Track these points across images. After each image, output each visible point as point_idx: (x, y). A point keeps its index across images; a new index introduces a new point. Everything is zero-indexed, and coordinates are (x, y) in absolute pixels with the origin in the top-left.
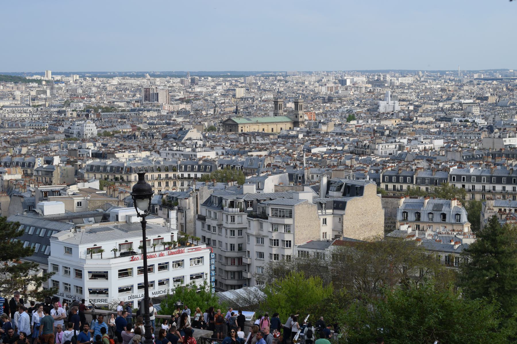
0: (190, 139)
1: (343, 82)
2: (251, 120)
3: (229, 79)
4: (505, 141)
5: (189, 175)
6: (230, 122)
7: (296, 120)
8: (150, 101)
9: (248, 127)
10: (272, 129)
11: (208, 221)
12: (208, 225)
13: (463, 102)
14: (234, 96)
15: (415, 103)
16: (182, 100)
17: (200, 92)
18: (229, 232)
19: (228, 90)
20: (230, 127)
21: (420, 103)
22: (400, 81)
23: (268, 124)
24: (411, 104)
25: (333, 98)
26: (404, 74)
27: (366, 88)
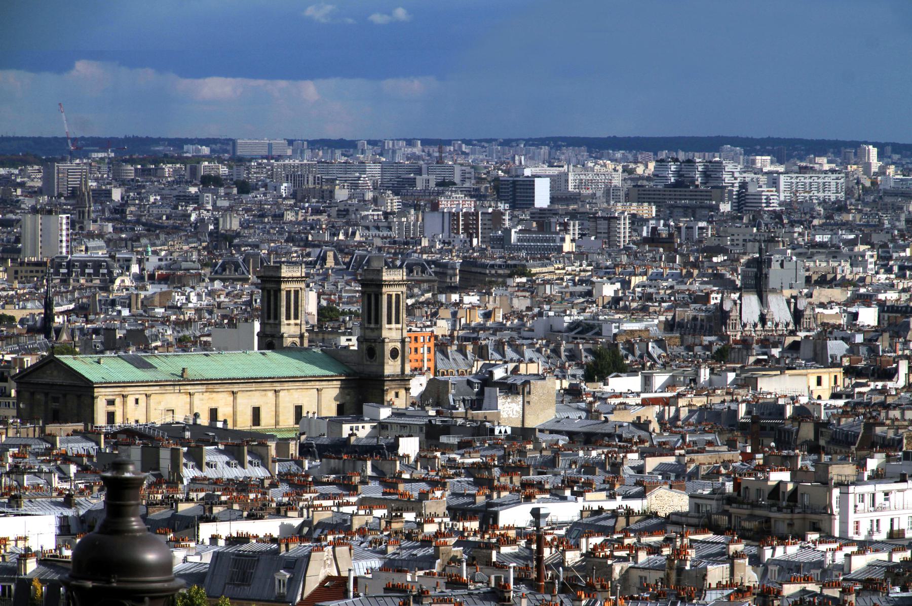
7: (370, 367)
10: (256, 412)
15: (881, 297)
23: (235, 388)
24: (866, 301)
25: (484, 266)
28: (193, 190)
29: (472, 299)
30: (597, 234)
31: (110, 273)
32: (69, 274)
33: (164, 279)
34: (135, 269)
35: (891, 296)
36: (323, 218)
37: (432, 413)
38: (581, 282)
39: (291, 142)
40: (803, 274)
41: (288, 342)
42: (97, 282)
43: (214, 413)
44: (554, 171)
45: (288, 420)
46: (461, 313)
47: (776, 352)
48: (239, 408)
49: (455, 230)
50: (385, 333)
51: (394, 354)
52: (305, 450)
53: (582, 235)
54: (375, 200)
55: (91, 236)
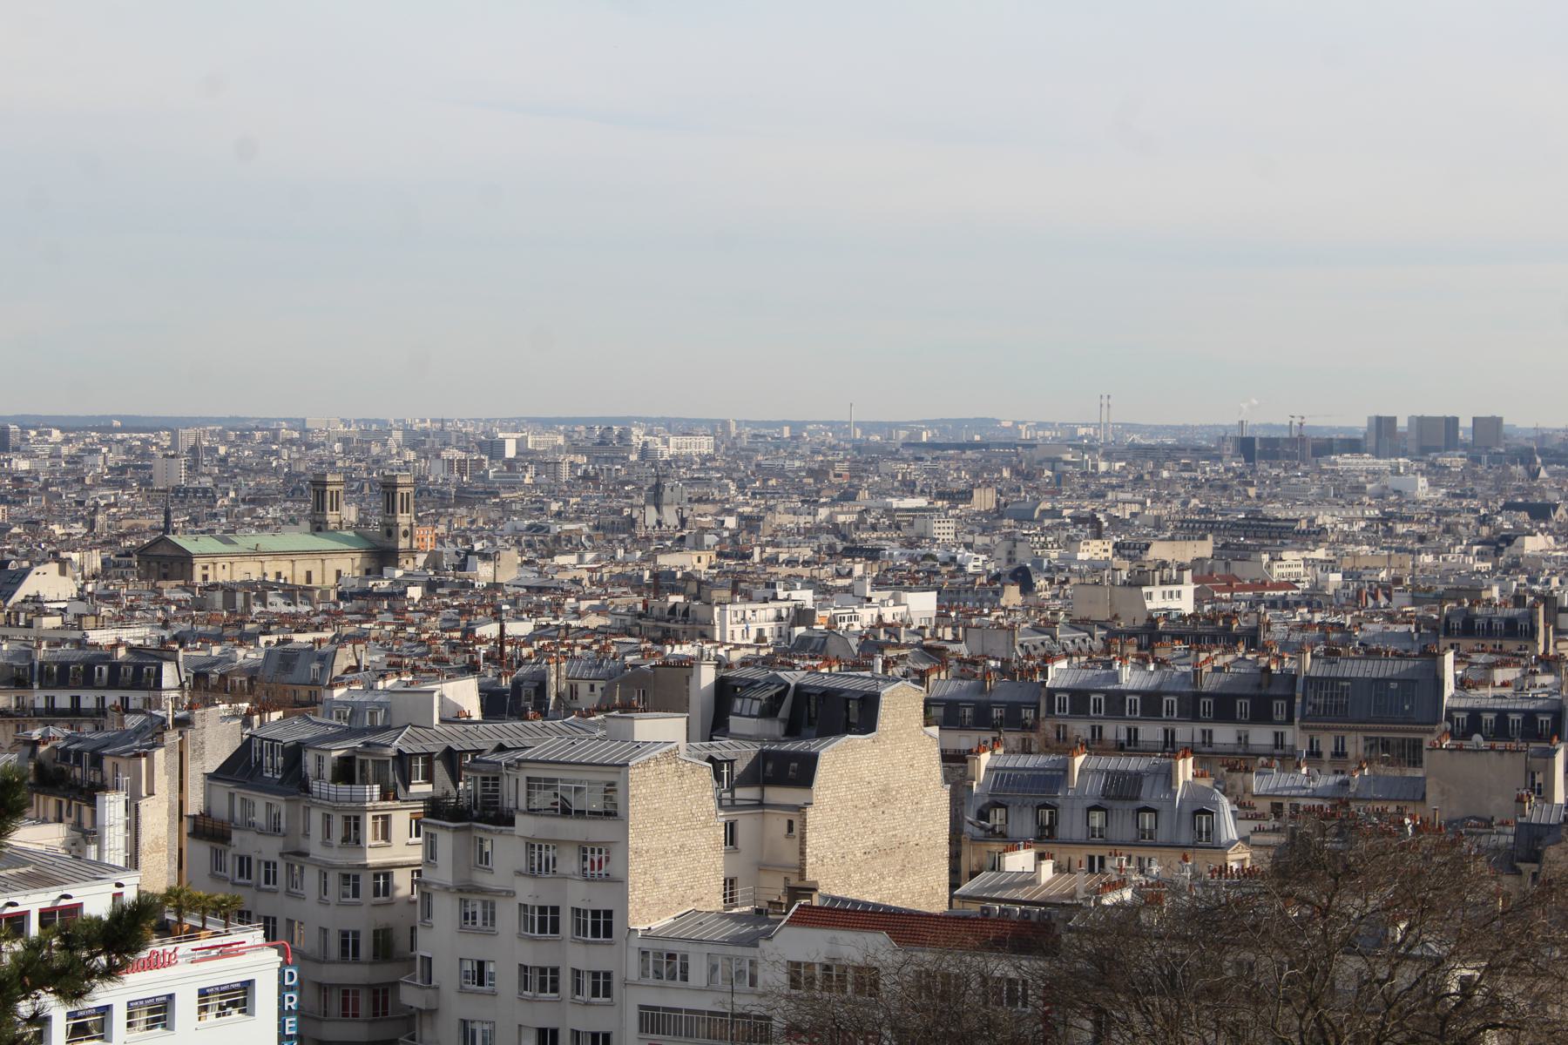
1: (494, 448)
2: (234, 543)
3: (119, 436)
5: (76, 700)
7: (389, 543)
10: (309, 574)
11: (242, 842)
13: (895, 506)
14: (146, 483)
15: (740, 510)
17: (29, 472)
18: (333, 879)
19: (122, 469)
20: (165, 566)
21: (756, 510)
22: (673, 450)
23: (294, 558)
24: (730, 512)
25: (471, 493)
28: (274, 447)
29: (463, 511)
30: (547, 473)
31: (214, 496)
32: (186, 497)
33: (252, 501)
34: (232, 494)
35: (747, 510)
36: (363, 465)
37: (431, 573)
38: (536, 502)
39: (342, 420)
40: (686, 496)
41: (331, 526)
42: (204, 501)
43: (279, 575)
44: (520, 435)
45: (331, 580)
46: (454, 520)
47: (669, 543)
48: (297, 572)
49: (451, 470)
50: (399, 520)
51: (405, 534)
52: (341, 596)
53: (537, 474)
54: (398, 454)
55: (203, 474)
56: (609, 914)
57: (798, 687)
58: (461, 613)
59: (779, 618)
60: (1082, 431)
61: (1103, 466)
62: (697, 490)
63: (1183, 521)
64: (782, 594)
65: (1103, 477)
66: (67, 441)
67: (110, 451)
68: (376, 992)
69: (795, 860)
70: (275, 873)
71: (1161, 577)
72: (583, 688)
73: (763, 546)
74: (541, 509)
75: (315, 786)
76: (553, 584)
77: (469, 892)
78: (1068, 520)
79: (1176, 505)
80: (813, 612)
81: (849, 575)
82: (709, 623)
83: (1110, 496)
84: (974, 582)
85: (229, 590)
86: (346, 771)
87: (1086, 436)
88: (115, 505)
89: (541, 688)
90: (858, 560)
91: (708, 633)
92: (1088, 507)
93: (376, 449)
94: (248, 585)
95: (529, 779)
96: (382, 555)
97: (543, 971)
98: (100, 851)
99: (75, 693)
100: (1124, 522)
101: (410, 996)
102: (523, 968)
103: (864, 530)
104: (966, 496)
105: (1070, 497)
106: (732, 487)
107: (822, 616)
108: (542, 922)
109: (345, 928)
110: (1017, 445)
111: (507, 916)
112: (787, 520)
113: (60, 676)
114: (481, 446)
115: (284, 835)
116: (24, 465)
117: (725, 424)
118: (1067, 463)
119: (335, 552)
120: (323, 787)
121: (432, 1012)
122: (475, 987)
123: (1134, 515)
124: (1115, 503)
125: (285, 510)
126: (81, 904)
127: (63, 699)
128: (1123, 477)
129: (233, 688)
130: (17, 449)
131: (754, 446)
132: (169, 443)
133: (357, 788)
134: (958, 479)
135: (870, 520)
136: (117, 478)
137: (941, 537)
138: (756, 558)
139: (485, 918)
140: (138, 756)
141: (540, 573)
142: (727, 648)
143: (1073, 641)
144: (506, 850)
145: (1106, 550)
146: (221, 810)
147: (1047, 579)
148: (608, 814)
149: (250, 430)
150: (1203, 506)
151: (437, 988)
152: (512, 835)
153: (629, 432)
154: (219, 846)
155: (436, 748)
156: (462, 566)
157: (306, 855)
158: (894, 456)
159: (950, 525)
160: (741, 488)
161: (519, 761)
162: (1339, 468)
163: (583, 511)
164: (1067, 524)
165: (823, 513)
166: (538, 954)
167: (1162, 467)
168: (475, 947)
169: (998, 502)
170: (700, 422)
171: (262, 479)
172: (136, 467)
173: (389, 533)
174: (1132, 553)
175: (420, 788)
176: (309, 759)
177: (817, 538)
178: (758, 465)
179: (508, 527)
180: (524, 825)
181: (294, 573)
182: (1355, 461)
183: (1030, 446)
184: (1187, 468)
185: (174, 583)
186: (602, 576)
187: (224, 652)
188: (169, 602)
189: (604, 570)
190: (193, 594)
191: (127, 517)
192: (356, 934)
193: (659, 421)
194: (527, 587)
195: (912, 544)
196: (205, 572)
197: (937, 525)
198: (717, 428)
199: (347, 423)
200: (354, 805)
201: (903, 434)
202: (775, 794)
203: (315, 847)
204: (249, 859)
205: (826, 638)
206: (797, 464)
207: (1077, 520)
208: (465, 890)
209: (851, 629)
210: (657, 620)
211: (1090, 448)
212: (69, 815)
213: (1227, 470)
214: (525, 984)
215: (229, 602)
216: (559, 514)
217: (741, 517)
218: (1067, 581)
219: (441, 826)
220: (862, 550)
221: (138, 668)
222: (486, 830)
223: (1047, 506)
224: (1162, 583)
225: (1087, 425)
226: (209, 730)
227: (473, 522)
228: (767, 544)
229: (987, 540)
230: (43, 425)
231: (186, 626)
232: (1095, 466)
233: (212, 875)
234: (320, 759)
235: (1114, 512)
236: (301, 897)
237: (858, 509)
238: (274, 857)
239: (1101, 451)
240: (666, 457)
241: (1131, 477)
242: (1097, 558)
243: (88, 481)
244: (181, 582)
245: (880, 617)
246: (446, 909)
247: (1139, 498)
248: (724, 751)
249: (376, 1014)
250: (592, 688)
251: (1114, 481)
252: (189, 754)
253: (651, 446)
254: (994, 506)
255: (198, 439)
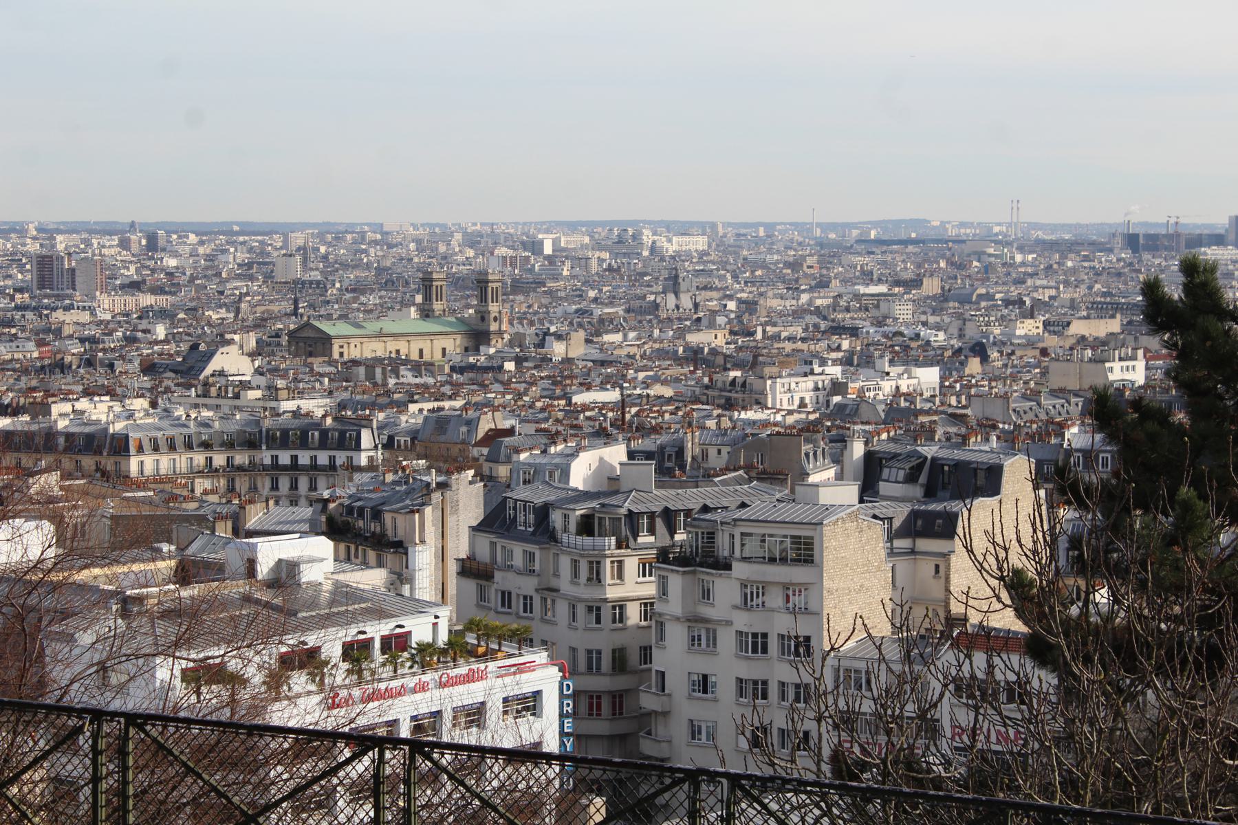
0: (222, 373)
1: (536, 247)
2: (363, 327)
3: (241, 239)
4: (1111, 370)
5: (294, 458)
6: (311, 334)
7: (482, 327)
8: (52, 289)
9: (359, 345)
10: (421, 351)
11: (502, 580)
12: (503, 593)
13: (862, 292)
14: (268, 277)
15: (738, 296)
16: (135, 286)
17: (177, 268)
18: (581, 610)
19: (249, 265)
20: (310, 346)
21: (751, 296)
22: (675, 247)
23: (409, 338)
24: (730, 298)
25: (523, 283)
26: (684, 229)
27: (601, 260)
28: (364, 247)
29: (520, 298)
30: (580, 267)
31: (325, 287)
32: (303, 287)
33: (354, 291)
34: (338, 285)
35: (744, 295)
36: (434, 260)
37: (518, 350)
38: (576, 290)
39: (412, 224)
40: (695, 284)
41: (437, 313)
42: (318, 291)
43: (398, 352)
44: (554, 236)
45: (438, 356)
46: (515, 306)
47: (688, 323)
49: (505, 264)
50: (490, 308)
51: (495, 319)
52: (453, 369)
53: (572, 268)
54: (460, 251)
55: (311, 269)
56: (808, 639)
57: (934, 459)
58: (555, 383)
59: (816, 389)
60: (996, 229)
61: (1019, 258)
62: (702, 280)
63: (1093, 303)
64: (817, 369)
65: (1020, 266)
66: (202, 243)
67: (236, 250)
68: (614, 697)
69: (941, 594)
70: (531, 604)
71: (1120, 355)
72: (712, 452)
73: (764, 325)
74: (581, 296)
75: (565, 538)
76: (611, 359)
77: (696, 621)
78: (1000, 303)
79: (1083, 289)
80: (846, 384)
81: (839, 348)
82: (763, 393)
83: (1029, 282)
84: (942, 355)
85: (370, 365)
86: (587, 526)
87: (1000, 233)
88: (247, 294)
89: (680, 452)
90: (844, 336)
91: (761, 401)
92: (1014, 292)
93: (442, 248)
94: (378, 361)
95: (742, 534)
96: (478, 336)
97: (755, 682)
98: (412, 590)
99: (294, 453)
100: (1045, 303)
101: (648, 701)
102: (740, 680)
103: (841, 311)
104: (916, 283)
105: (996, 283)
106: (729, 276)
107: (853, 386)
108: (755, 645)
109: (590, 647)
110: (946, 242)
111: (727, 641)
112: (775, 303)
113: (281, 439)
114: (524, 246)
115: (539, 575)
116: (172, 262)
117: (714, 226)
118: (990, 255)
119: (441, 334)
120: (570, 538)
121: (665, 714)
122: (701, 695)
123: (1051, 298)
124: (1036, 288)
125: (380, 297)
126: (410, 632)
127: (285, 458)
128: (1035, 266)
129: (399, 446)
130: (164, 250)
131: (738, 243)
132: (281, 244)
133: (598, 540)
134: (908, 270)
135: (843, 303)
136: (246, 271)
137: (902, 317)
138: (759, 336)
139: (708, 640)
140: (413, 512)
141: (601, 350)
142: (783, 413)
143: (1054, 407)
144: (725, 589)
145: (1038, 328)
146: (484, 554)
147: (998, 351)
148: (806, 561)
149: (342, 233)
150: (1105, 290)
151: (669, 695)
152: (729, 577)
153: (641, 233)
154: (483, 583)
155: (657, 508)
156: (541, 344)
157: (557, 590)
158: (849, 250)
159: (909, 307)
160: (735, 277)
161: (735, 520)
162: (1209, 257)
163: (614, 297)
164: (999, 306)
165: (805, 298)
166: (752, 670)
167: (1066, 258)
168: (701, 664)
169: (943, 288)
170: (692, 224)
171: (358, 273)
172: (259, 263)
173: (483, 319)
174: (1056, 329)
175: (645, 539)
176: (556, 517)
177: (803, 318)
178: (745, 259)
179: (559, 310)
180: (740, 570)
181: (409, 349)
182: (1221, 252)
183: (959, 241)
184: (1086, 259)
185: (321, 359)
186: (645, 351)
187: (388, 417)
188: (322, 375)
189: (646, 347)
190: (337, 368)
191: (259, 304)
192: (599, 652)
193: (660, 223)
194: (592, 361)
195: (880, 322)
196: (341, 350)
197: (898, 307)
198: (707, 228)
199: (415, 227)
200: (596, 552)
201: (855, 233)
202: (924, 544)
203: (564, 583)
204: (510, 593)
205: (858, 405)
206: (776, 257)
207: (1007, 303)
208: (693, 620)
209: (878, 398)
210: (721, 390)
211: (1008, 244)
212: (357, 557)
213: (1119, 260)
214: (741, 693)
215: (370, 376)
216: (595, 300)
217: (740, 301)
218: (1013, 353)
219: (672, 570)
220: (844, 328)
221: (342, 434)
222: (708, 574)
223: (982, 291)
224: (1121, 359)
225: (999, 224)
226: (461, 492)
227: (529, 307)
228: (767, 323)
229: (938, 319)
230: (181, 230)
231: (346, 395)
232: (1013, 258)
233: (478, 606)
234: (566, 516)
235: (1035, 295)
236: (554, 623)
237: (832, 294)
238: (531, 592)
239: (1015, 245)
240: (670, 253)
241: (1042, 267)
242: (1031, 333)
243: (224, 275)
244: (326, 359)
245: (897, 388)
246: (677, 635)
247: (1053, 284)
248: (884, 510)
249: (614, 714)
250: (719, 452)
251: (1029, 270)
252: (448, 510)
253: (658, 244)
254: (940, 291)
255: (306, 242)
